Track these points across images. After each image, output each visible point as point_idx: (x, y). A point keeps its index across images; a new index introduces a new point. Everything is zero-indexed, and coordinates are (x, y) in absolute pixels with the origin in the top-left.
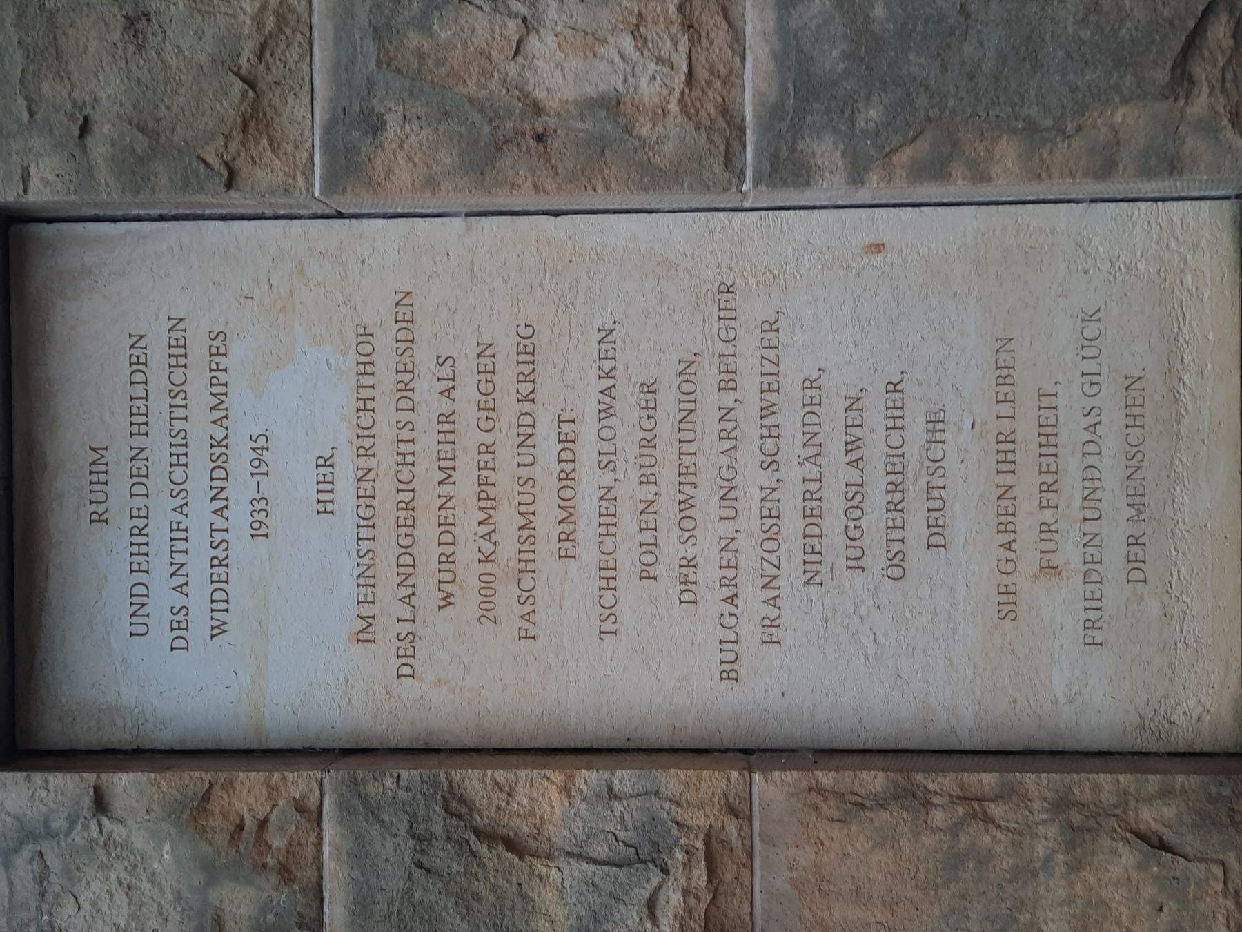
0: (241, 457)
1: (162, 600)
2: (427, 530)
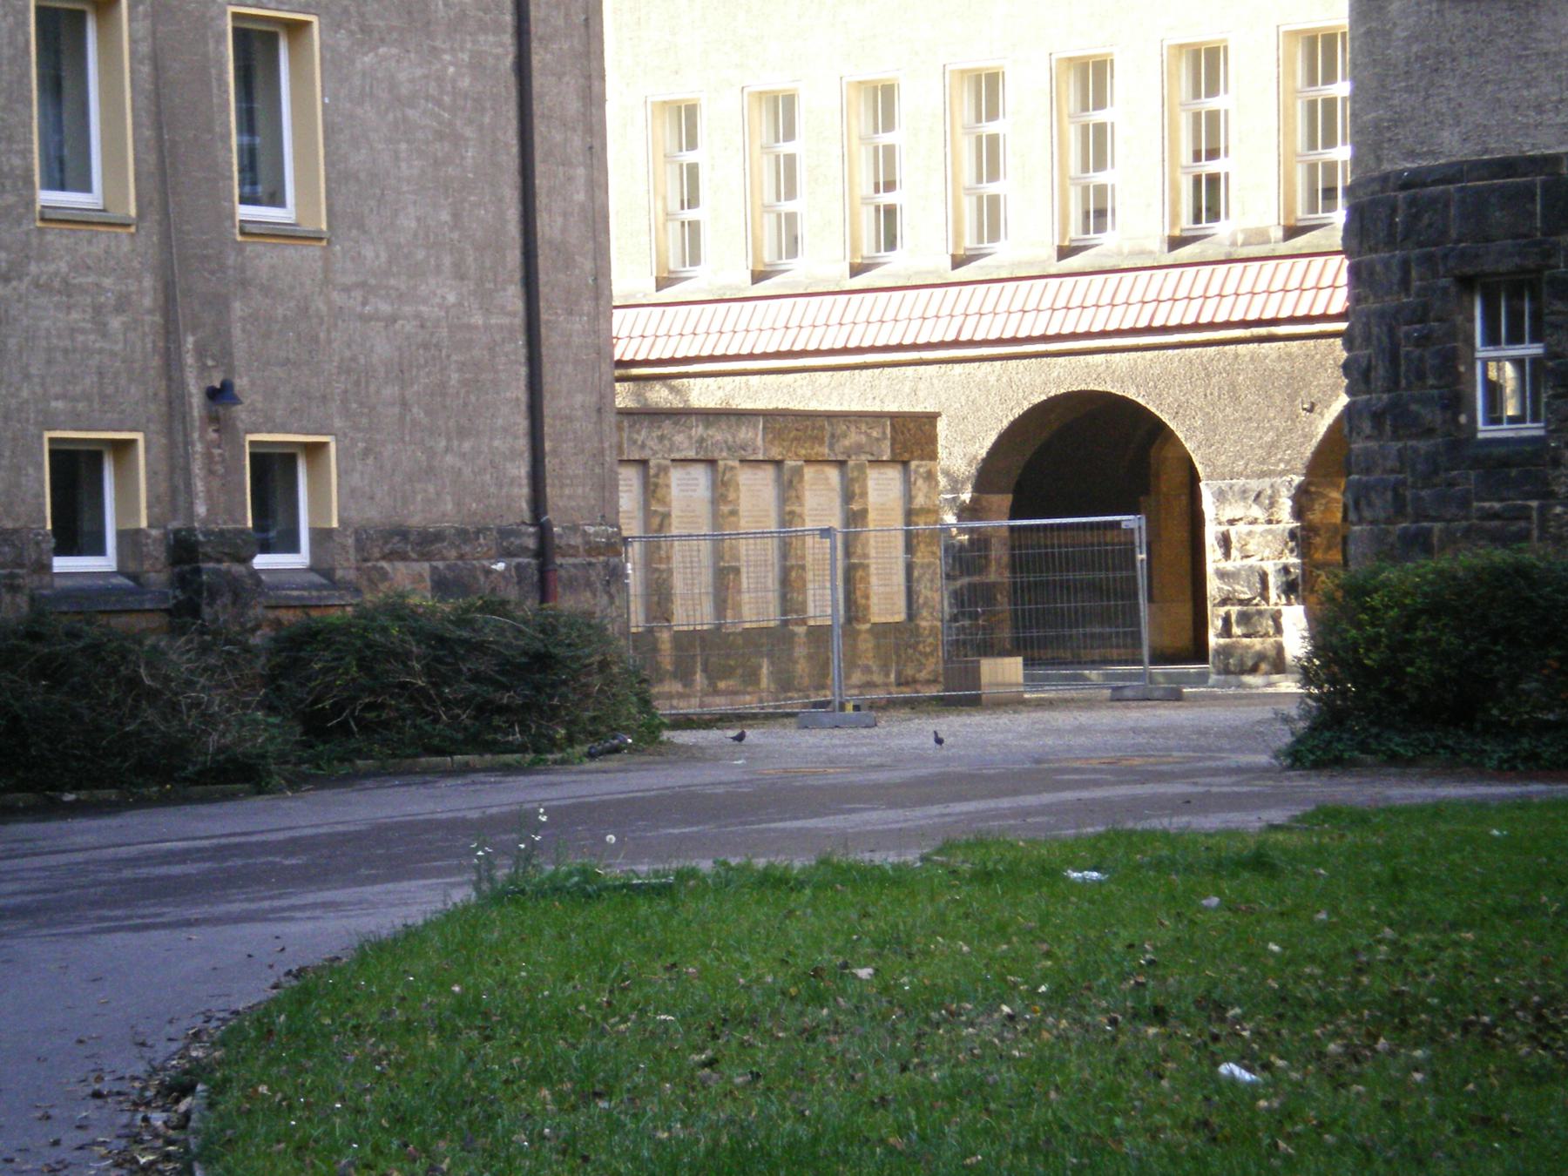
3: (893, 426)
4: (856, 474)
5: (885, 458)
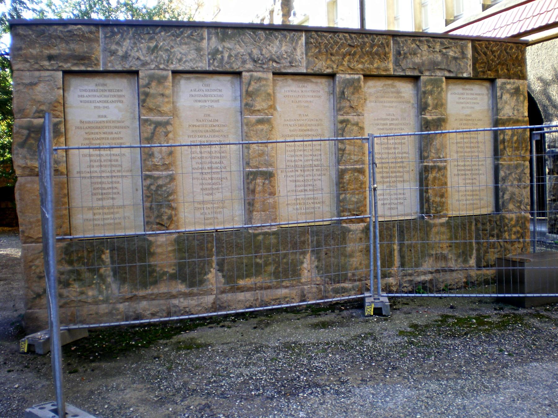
0: (106, 105)
1: (85, 94)
3: (474, 48)
4: (429, 88)
5: (465, 75)
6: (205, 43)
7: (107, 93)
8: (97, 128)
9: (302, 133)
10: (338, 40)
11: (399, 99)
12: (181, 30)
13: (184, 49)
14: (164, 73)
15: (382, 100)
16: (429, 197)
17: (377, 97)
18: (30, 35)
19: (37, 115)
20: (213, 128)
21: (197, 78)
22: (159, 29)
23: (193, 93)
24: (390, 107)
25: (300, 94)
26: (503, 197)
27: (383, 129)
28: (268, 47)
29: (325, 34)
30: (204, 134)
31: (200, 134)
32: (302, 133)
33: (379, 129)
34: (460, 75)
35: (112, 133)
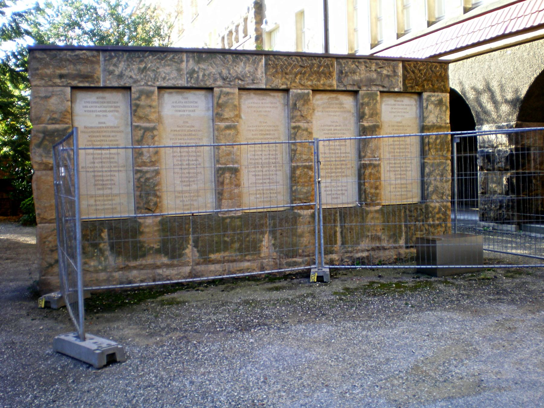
0: (105, 114)
1: (88, 105)
2: (98, 134)
3: (404, 67)
4: (366, 100)
5: (396, 90)
6: (184, 65)
7: (106, 105)
8: (98, 132)
9: (262, 137)
10: (292, 62)
11: (342, 109)
12: (165, 54)
13: (167, 69)
14: (152, 88)
15: (327, 110)
16: (365, 189)
17: (323, 108)
18: (45, 58)
19: (50, 122)
20: (190, 133)
21: (177, 93)
22: (147, 54)
23: (174, 105)
24: (334, 116)
25: (261, 105)
26: (428, 189)
27: (328, 134)
28: (235, 68)
29: (281, 57)
30: (183, 137)
31: (180, 137)
32: (262, 137)
33: (325, 134)
34: (392, 90)
35: (110, 136)
